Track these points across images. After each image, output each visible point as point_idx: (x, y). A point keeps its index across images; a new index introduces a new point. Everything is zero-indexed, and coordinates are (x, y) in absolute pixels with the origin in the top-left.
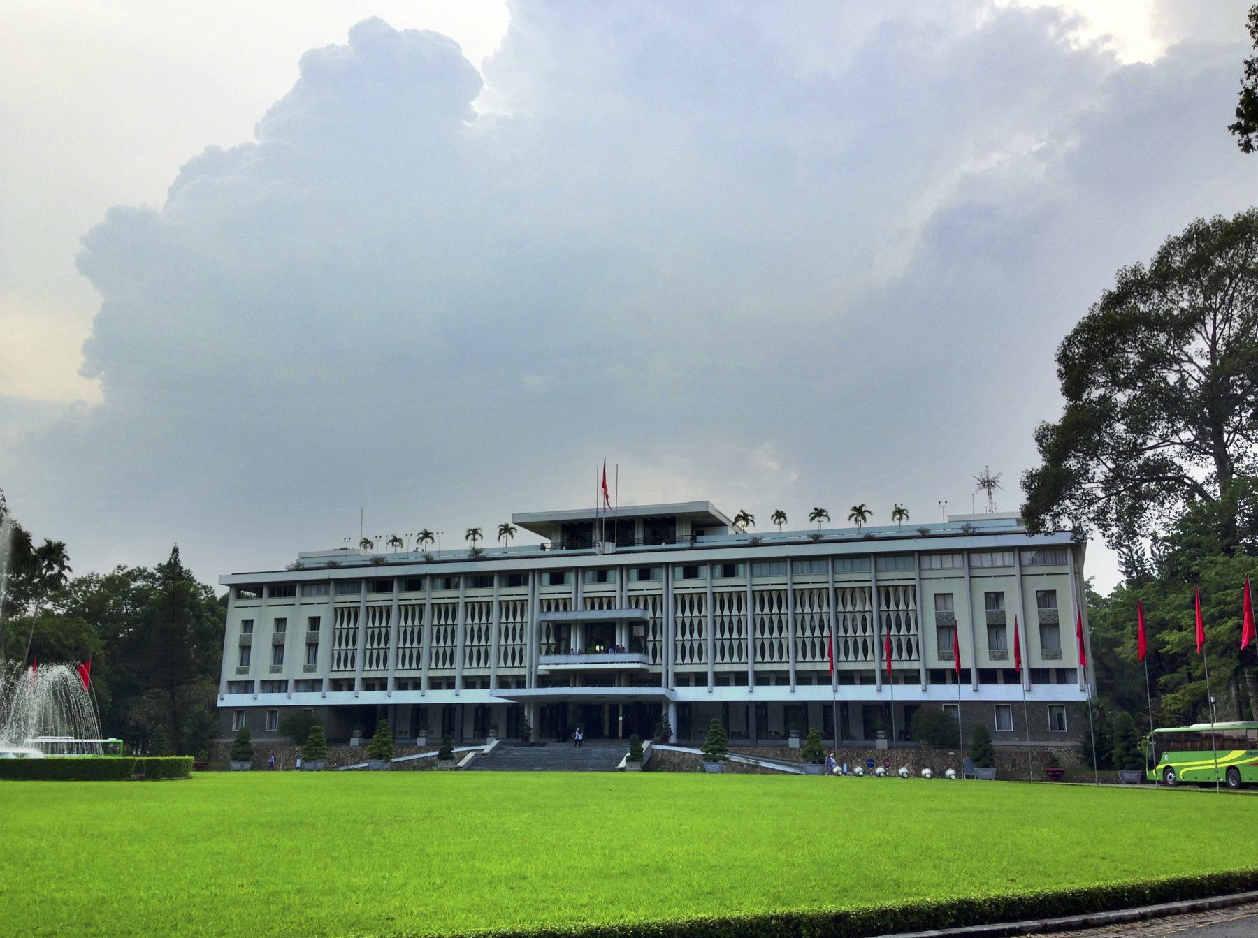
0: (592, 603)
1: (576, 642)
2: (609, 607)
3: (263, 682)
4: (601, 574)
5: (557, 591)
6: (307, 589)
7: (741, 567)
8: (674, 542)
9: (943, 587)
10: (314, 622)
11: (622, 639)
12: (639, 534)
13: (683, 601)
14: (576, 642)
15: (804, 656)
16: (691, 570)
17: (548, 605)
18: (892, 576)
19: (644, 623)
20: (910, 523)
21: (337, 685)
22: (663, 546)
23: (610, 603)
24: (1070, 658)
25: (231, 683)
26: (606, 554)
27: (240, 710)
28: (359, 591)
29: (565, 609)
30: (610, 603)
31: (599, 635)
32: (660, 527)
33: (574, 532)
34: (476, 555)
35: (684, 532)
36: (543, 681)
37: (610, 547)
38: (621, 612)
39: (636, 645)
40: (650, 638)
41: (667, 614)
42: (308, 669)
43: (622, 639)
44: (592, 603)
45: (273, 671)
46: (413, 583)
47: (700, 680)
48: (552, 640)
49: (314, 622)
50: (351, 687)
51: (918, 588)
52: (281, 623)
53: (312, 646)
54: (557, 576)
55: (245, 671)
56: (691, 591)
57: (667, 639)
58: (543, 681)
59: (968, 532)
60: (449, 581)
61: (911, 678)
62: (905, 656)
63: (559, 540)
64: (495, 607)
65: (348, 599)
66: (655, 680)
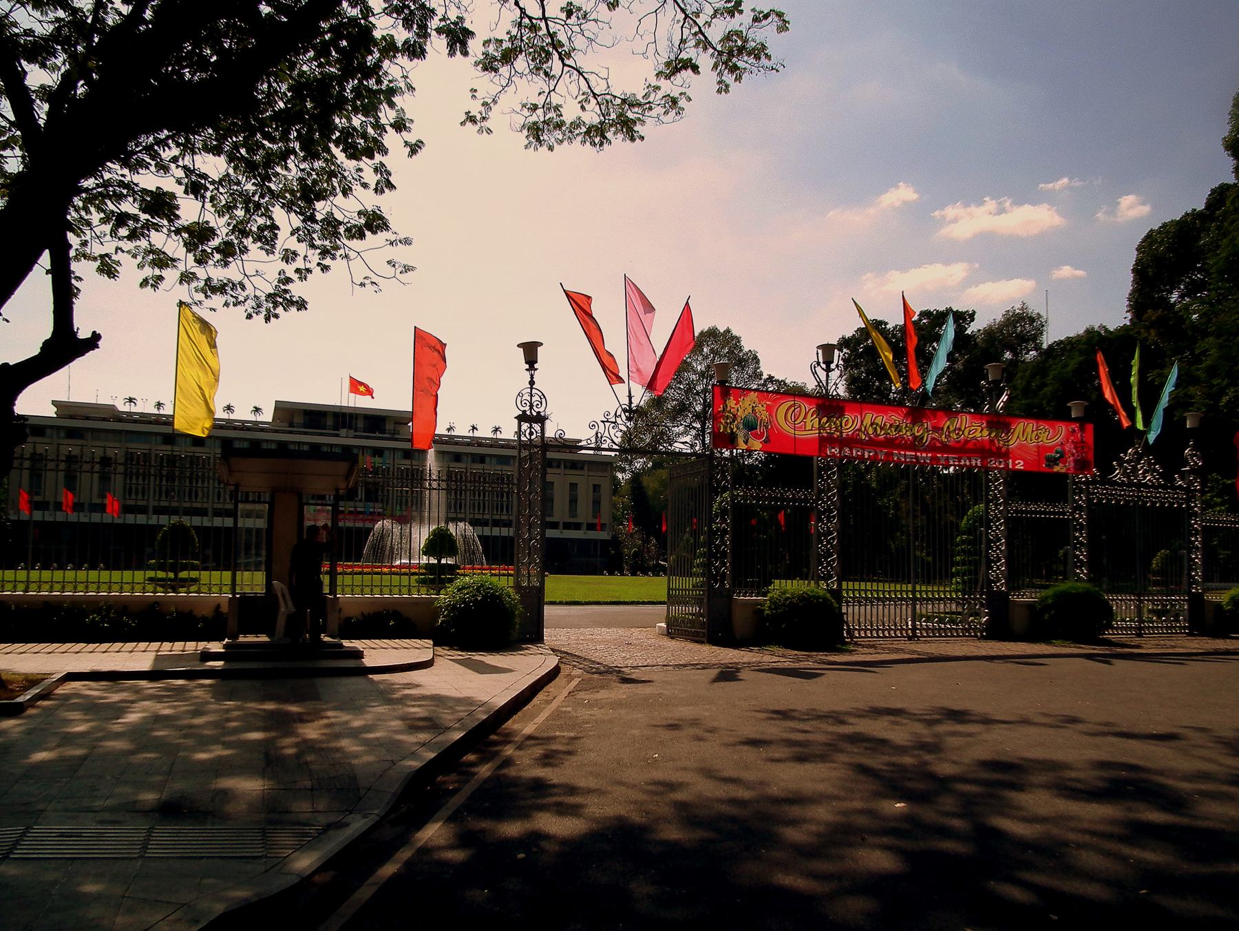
12: (361, 424)
22: (377, 434)
26: (345, 439)
35: (389, 426)
37: (352, 433)
43: (361, 493)
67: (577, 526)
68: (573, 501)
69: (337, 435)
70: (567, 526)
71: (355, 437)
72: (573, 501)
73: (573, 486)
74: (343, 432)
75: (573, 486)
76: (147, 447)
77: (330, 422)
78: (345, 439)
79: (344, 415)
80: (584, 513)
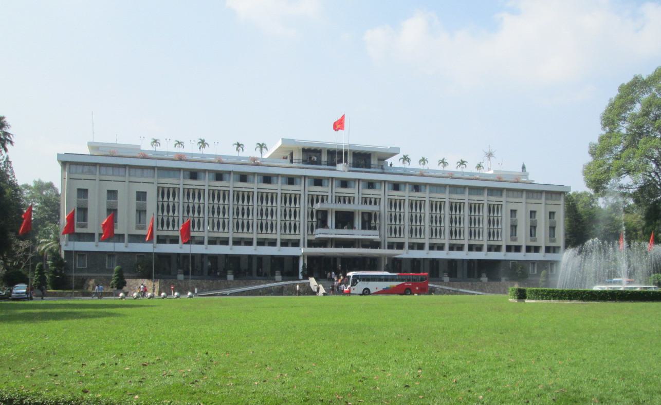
0: (339, 199)
1: (331, 220)
2: (349, 202)
4: (344, 183)
5: (318, 190)
7: (227, 176)
8: (369, 167)
10: (141, 196)
11: (358, 221)
12: (350, 159)
13: (392, 203)
14: (331, 220)
15: (416, 235)
16: (396, 186)
17: (313, 200)
18: (494, 199)
19: (369, 214)
20: (410, 167)
23: (350, 200)
26: (342, 170)
28: (179, 178)
30: (350, 200)
31: (345, 219)
32: (362, 159)
33: (311, 155)
34: (255, 162)
35: (374, 162)
40: (373, 222)
41: (383, 208)
42: (138, 228)
43: (358, 221)
44: (339, 199)
47: (400, 246)
48: (315, 219)
49: (141, 196)
50: (202, 243)
51: (503, 207)
52: (112, 194)
53: (141, 212)
54: (318, 182)
56: (396, 198)
57: (385, 223)
58: (311, 244)
59: (499, 180)
61: (498, 248)
62: (418, 236)
63: (301, 158)
64: (427, 204)
66: (375, 245)
67: (537, 249)
68: (533, 228)
69: (335, 170)
70: (529, 249)
71: (349, 171)
72: (533, 228)
73: (533, 213)
74: (340, 167)
75: (533, 213)
76: (175, 181)
77: (324, 158)
78: (342, 170)
79: (340, 153)
80: (542, 240)
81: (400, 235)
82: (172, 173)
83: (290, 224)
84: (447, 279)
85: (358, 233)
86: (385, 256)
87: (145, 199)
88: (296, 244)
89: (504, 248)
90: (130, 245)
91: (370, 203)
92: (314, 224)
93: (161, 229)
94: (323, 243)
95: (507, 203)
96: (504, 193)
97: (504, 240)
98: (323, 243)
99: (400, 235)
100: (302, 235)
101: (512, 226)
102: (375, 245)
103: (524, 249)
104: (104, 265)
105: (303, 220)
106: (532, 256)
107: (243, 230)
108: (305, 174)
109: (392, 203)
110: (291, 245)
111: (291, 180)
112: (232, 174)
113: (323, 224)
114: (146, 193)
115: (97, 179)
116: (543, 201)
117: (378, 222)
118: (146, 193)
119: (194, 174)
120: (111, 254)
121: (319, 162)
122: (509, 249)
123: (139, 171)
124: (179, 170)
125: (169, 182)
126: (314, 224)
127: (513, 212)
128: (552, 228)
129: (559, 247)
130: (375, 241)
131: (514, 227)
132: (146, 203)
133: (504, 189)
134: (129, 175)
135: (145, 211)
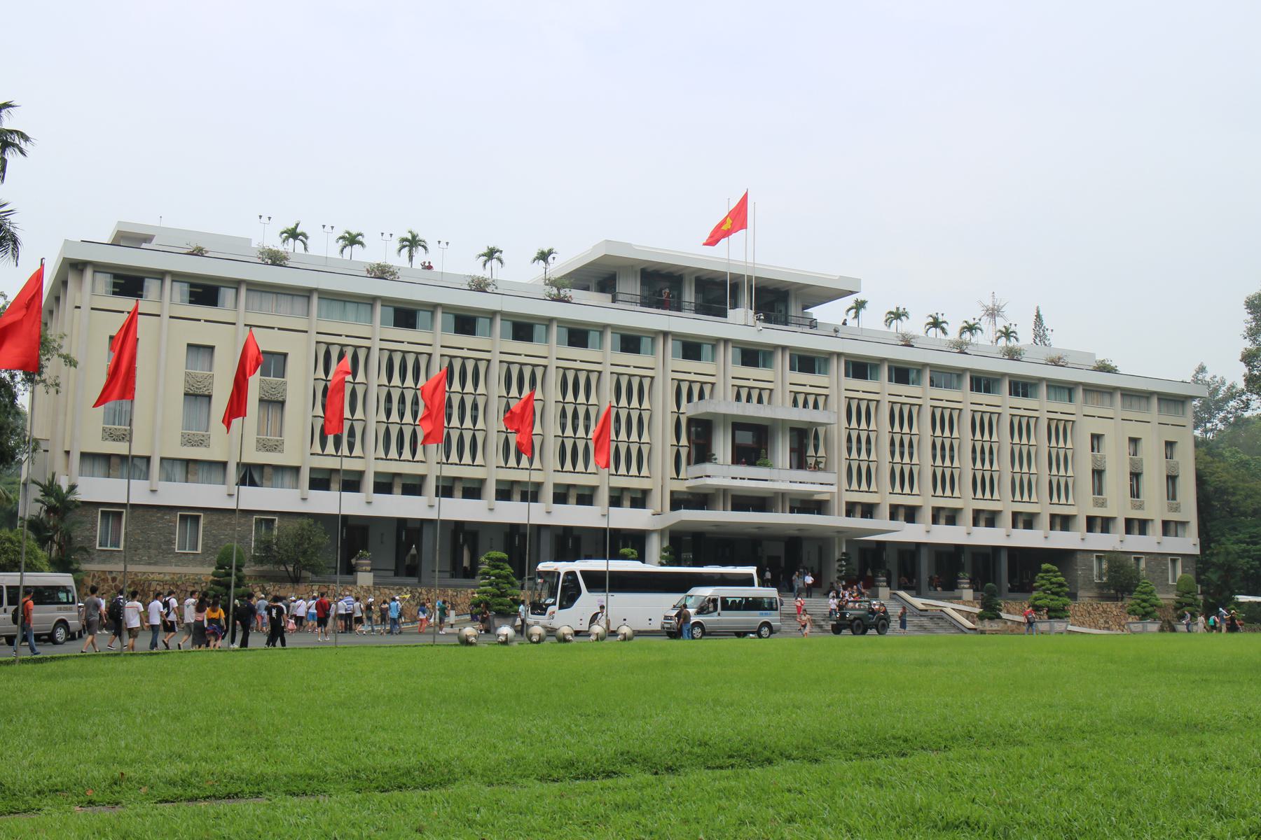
3: (162, 459)
4: (752, 355)
6: (256, 297)
9: (1097, 427)
14: (722, 447)
16: (860, 368)
18: (1061, 407)
21: (320, 481)
24: (1188, 509)
25: (84, 455)
26: (741, 324)
27: (112, 512)
29: (701, 396)
31: (753, 444)
36: (678, 502)
38: (780, 410)
39: (800, 461)
40: (811, 452)
45: (189, 441)
46: (465, 323)
51: (1077, 424)
54: (691, 349)
55: (127, 437)
57: (840, 456)
60: (523, 329)
65: (348, 328)
66: (818, 506)
81: (639, 470)
82: (350, 307)
83: (461, 438)
84: (968, 594)
85: (779, 476)
86: (840, 531)
87: (282, 374)
88: (640, 500)
89: (1082, 523)
90: (163, 486)
91: (805, 405)
92: (684, 452)
93: (346, 452)
94: (701, 500)
95: (1088, 418)
96: (1043, 389)
97: (1082, 505)
98: (701, 500)
99: (639, 470)
100: (660, 477)
101: (1093, 471)
102: (818, 506)
103: (1121, 525)
104: (171, 542)
105: (662, 440)
106: (1135, 543)
107: (574, 464)
108: (665, 329)
109: (858, 411)
110: (519, 497)
111: (630, 342)
112: (498, 320)
113: (702, 453)
114: (285, 355)
115: (165, 316)
116: (1154, 412)
117: (821, 452)
118: (285, 355)
119: (406, 316)
120: (190, 516)
121: (675, 305)
122: (1091, 523)
123: (269, 301)
124: (371, 301)
125: (348, 328)
126: (684, 452)
127: (1096, 438)
128: (1172, 479)
129: (1184, 524)
130: (817, 497)
131: (1098, 473)
132: (285, 383)
133: (1077, 384)
134: (246, 308)
135: (282, 403)
